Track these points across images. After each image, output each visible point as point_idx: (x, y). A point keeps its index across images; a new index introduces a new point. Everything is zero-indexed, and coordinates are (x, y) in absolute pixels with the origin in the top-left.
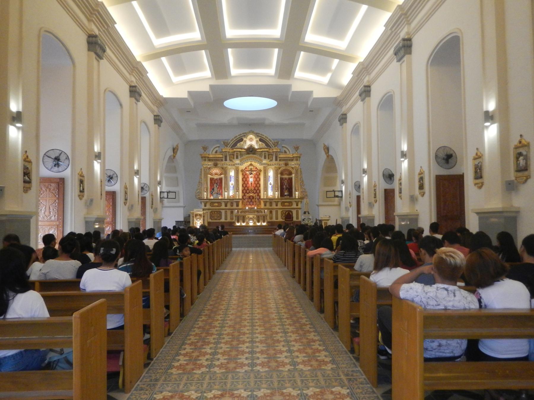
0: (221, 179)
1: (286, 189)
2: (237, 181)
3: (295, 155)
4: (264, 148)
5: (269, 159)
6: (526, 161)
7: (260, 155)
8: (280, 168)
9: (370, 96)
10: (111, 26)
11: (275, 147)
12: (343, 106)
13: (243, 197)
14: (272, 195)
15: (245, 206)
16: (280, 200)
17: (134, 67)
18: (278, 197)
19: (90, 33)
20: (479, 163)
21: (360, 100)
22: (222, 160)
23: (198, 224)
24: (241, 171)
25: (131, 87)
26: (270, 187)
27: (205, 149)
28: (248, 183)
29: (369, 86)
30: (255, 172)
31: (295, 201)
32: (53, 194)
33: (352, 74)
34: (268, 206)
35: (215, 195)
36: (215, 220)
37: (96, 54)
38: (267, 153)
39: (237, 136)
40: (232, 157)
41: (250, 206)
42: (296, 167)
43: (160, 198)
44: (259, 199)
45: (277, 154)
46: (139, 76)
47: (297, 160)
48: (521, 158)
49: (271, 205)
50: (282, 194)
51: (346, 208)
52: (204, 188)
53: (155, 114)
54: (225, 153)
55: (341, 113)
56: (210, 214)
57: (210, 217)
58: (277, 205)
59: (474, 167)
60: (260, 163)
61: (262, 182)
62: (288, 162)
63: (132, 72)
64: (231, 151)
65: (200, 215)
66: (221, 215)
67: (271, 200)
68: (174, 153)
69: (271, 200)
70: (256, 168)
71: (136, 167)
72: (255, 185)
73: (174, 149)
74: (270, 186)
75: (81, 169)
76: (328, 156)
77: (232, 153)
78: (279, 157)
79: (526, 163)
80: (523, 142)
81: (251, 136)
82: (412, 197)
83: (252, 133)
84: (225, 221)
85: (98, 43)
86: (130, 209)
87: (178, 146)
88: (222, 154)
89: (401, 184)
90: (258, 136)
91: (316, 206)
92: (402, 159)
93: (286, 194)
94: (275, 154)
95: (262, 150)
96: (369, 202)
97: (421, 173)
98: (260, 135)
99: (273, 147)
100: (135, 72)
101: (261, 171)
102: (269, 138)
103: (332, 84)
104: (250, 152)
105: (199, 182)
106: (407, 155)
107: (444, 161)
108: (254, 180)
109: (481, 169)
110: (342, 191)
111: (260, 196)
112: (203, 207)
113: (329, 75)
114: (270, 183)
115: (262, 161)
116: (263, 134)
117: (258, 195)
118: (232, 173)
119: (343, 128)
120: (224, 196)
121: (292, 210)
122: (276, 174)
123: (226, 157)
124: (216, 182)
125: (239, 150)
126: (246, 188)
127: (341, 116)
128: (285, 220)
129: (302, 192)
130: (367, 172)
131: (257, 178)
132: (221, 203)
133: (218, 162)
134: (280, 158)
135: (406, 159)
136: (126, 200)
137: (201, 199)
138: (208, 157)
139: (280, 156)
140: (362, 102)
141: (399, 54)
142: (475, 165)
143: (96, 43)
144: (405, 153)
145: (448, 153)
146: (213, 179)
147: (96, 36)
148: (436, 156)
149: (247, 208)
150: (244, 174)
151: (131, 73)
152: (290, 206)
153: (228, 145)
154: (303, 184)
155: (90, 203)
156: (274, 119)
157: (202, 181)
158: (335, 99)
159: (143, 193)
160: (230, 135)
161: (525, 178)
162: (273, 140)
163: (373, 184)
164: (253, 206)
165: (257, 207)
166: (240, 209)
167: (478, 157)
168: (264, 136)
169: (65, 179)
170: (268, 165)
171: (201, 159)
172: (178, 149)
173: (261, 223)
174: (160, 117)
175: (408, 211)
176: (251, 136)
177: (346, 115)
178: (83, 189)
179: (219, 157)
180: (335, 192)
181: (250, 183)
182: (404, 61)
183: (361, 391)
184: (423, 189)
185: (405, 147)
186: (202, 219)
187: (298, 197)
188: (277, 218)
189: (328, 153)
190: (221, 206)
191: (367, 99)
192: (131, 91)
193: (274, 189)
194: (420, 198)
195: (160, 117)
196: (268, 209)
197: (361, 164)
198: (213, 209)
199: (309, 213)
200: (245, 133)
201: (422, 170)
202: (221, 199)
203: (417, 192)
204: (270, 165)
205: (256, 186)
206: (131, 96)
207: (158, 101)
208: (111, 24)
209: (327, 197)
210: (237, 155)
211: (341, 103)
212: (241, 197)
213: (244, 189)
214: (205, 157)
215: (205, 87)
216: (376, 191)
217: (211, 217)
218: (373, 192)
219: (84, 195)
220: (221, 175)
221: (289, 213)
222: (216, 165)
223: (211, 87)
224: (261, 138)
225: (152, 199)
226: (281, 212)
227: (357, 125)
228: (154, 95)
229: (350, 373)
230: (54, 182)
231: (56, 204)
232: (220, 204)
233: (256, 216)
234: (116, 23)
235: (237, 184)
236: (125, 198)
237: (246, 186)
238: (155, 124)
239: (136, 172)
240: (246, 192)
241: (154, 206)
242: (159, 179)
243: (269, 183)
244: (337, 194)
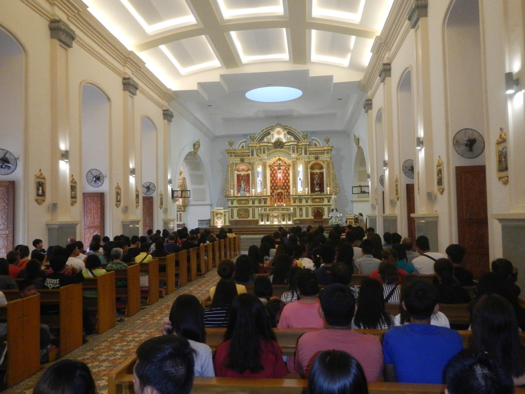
0: (248, 176)
1: (317, 184)
2: (265, 177)
3: (326, 148)
4: (292, 142)
5: (297, 152)
7: (289, 149)
8: (309, 162)
9: (390, 76)
10: (82, 10)
11: (304, 140)
12: (368, 90)
13: (271, 193)
14: (302, 191)
15: (274, 203)
16: (310, 196)
17: (126, 58)
18: (308, 193)
19: (52, 18)
20: (503, 149)
22: (249, 156)
23: (219, 224)
24: (269, 166)
25: (124, 79)
26: (299, 183)
27: (231, 144)
28: (276, 179)
29: (389, 64)
30: (283, 167)
31: (327, 197)
32: (2, 199)
33: (371, 52)
34: (297, 203)
35: (242, 192)
36: (242, 218)
37: (60, 40)
38: (295, 147)
39: (264, 130)
40: (259, 152)
41: (279, 204)
43: (173, 197)
44: (288, 195)
45: (307, 147)
46: (137, 68)
47: (328, 153)
49: (301, 201)
50: (313, 190)
51: (372, 205)
52: (231, 185)
53: (165, 109)
54: (252, 148)
56: (237, 212)
57: (238, 215)
58: (307, 202)
59: (498, 154)
60: (288, 157)
61: (291, 178)
62: (319, 155)
63: (125, 63)
64: (258, 145)
65: (221, 214)
66: (249, 213)
67: (301, 197)
68: (194, 149)
69: (301, 197)
70: (285, 163)
71: (132, 166)
72: (284, 181)
73: (194, 145)
74: (300, 181)
75: (40, 170)
76: (358, 148)
77: (259, 148)
78: (309, 151)
81: (279, 129)
82: (429, 195)
83: (279, 125)
84: (254, 219)
85: (61, 30)
86: (124, 210)
87: (199, 142)
88: (249, 149)
89: (418, 178)
90: (285, 128)
91: (350, 202)
92: (418, 148)
93: (317, 189)
94: (305, 147)
95: (290, 144)
96: (390, 200)
98: (288, 128)
99: (302, 140)
100: (128, 62)
101: (290, 166)
102: (298, 131)
103: (354, 66)
104: (278, 146)
105: (226, 179)
107: (467, 148)
108: (282, 176)
109: (505, 157)
110: (369, 186)
111: (289, 193)
112: (230, 204)
113: (349, 56)
114: (300, 178)
115: (290, 155)
116: (292, 126)
117: (287, 191)
118: (260, 169)
119: (368, 115)
120: (252, 193)
121: (324, 207)
122: (306, 169)
123: (252, 152)
124: (244, 178)
125: (267, 144)
126: (275, 185)
128: (315, 218)
129: (334, 188)
131: (286, 173)
132: (249, 201)
133: (244, 158)
134: (311, 152)
135: (422, 148)
136: (118, 201)
137: (228, 196)
138: (234, 153)
139: (310, 149)
141: (413, 17)
142: (499, 152)
143: (59, 29)
144: (421, 140)
145: (470, 138)
146: (240, 175)
147: (59, 21)
149: (276, 205)
150: (272, 169)
151: (124, 64)
152: (321, 203)
153: (255, 139)
154: (335, 178)
155: (54, 207)
156: (302, 110)
157: (228, 178)
158: (359, 83)
159: (149, 193)
160: (257, 129)
162: (303, 132)
163: (395, 179)
164: (282, 204)
165: (286, 204)
166: (268, 206)
167: (502, 141)
168: (292, 128)
169: (15, 183)
170: (297, 159)
171: (227, 154)
172: (199, 146)
173: (287, 221)
174: (169, 112)
175: (425, 213)
176: (279, 129)
177: (371, 100)
178: (43, 192)
179: (245, 153)
180: (362, 188)
181: (278, 179)
182: (418, 27)
184: (441, 184)
185: (421, 133)
186: (223, 218)
187: (330, 192)
188: (307, 215)
189: (359, 144)
190: (249, 203)
192: (124, 84)
193: (304, 185)
194: (439, 195)
195: (169, 111)
196: (298, 206)
198: (240, 207)
199: (337, 211)
200: (273, 126)
201: (440, 160)
202: (248, 197)
203: (435, 188)
204: (300, 159)
205: (285, 182)
206: (124, 89)
207: (167, 95)
208: (81, 8)
210: (264, 149)
211: (366, 87)
212: (269, 194)
213: (273, 185)
214: (231, 153)
215: (214, 78)
216: (398, 186)
217: (239, 215)
218: (395, 189)
219: (45, 199)
220: (248, 171)
221: (318, 211)
222: (242, 161)
223: (222, 76)
224: (289, 130)
225: (161, 199)
226: (312, 209)
228: (161, 89)
230: (4, 186)
231: (6, 211)
232: (247, 201)
233: (281, 214)
234: (88, 7)
235: (264, 180)
236: (117, 199)
237: (275, 182)
238: (164, 119)
239: (132, 170)
240: (275, 188)
241: (164, 207)
242: (169, 177)
243: (298, 178)
244: (364, 189)
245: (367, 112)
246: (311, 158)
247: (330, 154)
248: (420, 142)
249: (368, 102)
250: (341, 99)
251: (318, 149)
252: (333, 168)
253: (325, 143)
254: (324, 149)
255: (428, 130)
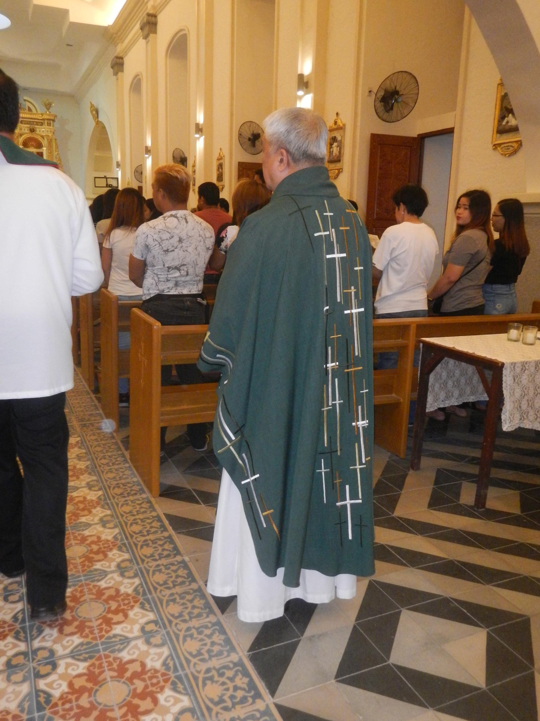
3: (45, 117)
6: (340, 149)
9: (155, 32)
12: (118, 43)
21: (142, 38)
42: (48, 136)
47: (49, 124)
48: (335, 144)
55: (116, 55)
62: (36, 126)
79: (340, 152)
80: (340, 123)
92: (197, 136)
97: (220, 157)
106: (204, 130)
110: (117, 179)
119: (117, 79)
127: (115, 59)
130: (151, 151)
135: (201, 136)
140: (144, 40)
144: (200, 127)
145: (255, 132)
148: (240, 135)
161: (337, 171)
177: (122, 58)
183: (95, 437)
185: (200, 118)
189: (98, 118)
191: (152, 36)
197: (143, 140)
201: (221, 153)
209: (95, 187)
211: (114, 38)
227: (138, 77)
229: (87, 418)
245: (116, 74)
246: (23, 129)
247: (53, 126)
248: (199, 129)
249: (118, 60)
250: (72, 46)
251: (34, 117)
252: (57, 147)
253: (46, 110)
254: (43, 117)
255: (208, 115)
